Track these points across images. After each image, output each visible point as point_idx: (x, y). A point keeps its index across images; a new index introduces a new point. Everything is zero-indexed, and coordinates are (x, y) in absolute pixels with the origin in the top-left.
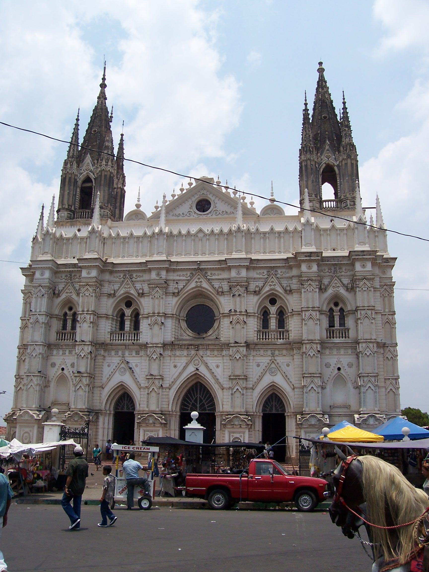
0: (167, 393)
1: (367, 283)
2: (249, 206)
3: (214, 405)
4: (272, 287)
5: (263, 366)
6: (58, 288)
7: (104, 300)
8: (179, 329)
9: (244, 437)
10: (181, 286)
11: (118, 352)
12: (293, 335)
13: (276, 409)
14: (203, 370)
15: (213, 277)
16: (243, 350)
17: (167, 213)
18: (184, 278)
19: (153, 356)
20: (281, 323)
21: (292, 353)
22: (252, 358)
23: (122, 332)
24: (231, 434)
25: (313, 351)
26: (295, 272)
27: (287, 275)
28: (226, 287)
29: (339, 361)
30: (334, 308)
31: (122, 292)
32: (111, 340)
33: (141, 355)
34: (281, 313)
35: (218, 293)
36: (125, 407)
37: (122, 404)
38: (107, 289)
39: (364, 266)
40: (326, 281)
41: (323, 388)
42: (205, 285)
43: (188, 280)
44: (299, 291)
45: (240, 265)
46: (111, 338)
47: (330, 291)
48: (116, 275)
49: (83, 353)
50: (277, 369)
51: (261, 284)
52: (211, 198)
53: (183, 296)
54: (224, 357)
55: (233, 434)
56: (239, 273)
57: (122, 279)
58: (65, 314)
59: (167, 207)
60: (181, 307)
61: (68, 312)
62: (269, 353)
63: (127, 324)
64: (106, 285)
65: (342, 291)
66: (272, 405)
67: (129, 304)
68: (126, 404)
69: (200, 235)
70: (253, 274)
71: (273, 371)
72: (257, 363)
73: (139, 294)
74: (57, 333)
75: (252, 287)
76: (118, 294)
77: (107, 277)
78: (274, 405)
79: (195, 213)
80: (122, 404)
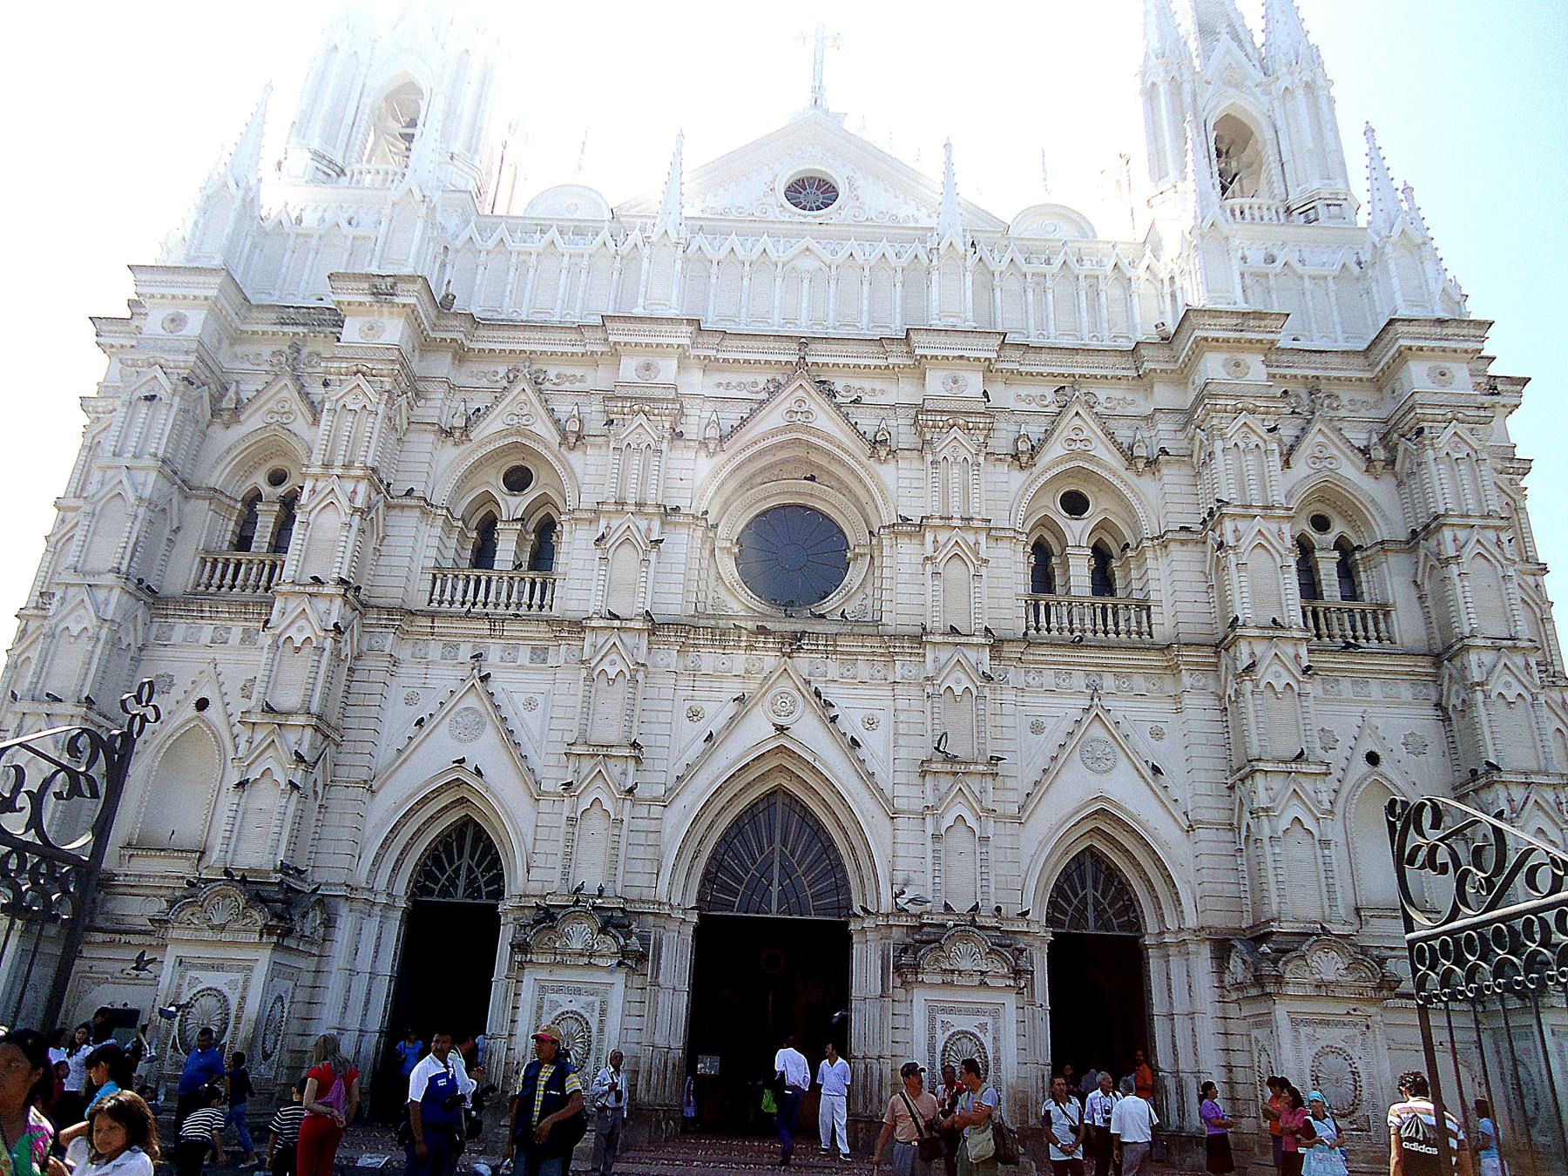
0: (653, 825)
3: (842, 886)
6: (237, 393)
7: (423, 443)
8: (712, 583)
9: (997, 1030)
11: (457, 647)
13: (1098, 917)
14: (809, 733)
18: (745, 394)
19: (605, 666)
22: (1010, 696)
23: (483, 574)
24: (940, 1017)
25: (1282, 670)
30: (1315, 536)
31: (498, 425)
32: (431, 601)
33: (551, 661)
36: (462, 883)
37: (449, 871)
38: (438, 406)
43: (762, 402)
45: (961, 357)
46: (432, 594)
48: (476, 367)
49: (300, 630)
50: (1118, 750)
51: (1035, 430)
54: (899, 689)
55: (946, 1017)
57: (504, 383)
58: (255, 498)
63: (506, 549)
64: (437, 393)
65: (1350, 471)
66: (1084, 900)
67: (518, 480)
68: (463, 873)
71: (1099, 754)
72: (1034, 719)
73: (564, 435)
74: (204, 561)
76: (480, 432)
78: (1090, 900)
80: (449, 871)
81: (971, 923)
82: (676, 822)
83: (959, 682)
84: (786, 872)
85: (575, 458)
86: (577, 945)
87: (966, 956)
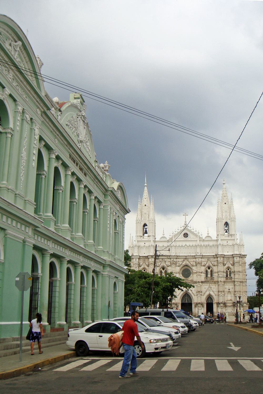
1: (238, 264)
2: (201, 236)
4: (209, 264)
5: (206, 289)
10: (181, 263)
12: (216, 279)
15: (190, 261)
16: (201, 284)
20: (212, 275)
22: (203, 286)
26: (216, 259)
28: (195, 264)
29: (229, 287)
30: (228, 271)
34: (211, 271)
35: (192, 266)
39: (237, 259)
41: (224, 295)
44: (217, 265)
47: (227, 266)
51: (205, 263)
52: (188, 233)
53: (182, 266)
56: (199, 260)
59: (174, 236)
62: (208, 284)
65: (230, 266)
69: (186, 246)
70: (203, 260)
73: (167, 266)
75: (203, 264)
76: (160, 266)
79: (183, 238)
81: (199, 303)
83: (199, 285)
87: (199, 305)
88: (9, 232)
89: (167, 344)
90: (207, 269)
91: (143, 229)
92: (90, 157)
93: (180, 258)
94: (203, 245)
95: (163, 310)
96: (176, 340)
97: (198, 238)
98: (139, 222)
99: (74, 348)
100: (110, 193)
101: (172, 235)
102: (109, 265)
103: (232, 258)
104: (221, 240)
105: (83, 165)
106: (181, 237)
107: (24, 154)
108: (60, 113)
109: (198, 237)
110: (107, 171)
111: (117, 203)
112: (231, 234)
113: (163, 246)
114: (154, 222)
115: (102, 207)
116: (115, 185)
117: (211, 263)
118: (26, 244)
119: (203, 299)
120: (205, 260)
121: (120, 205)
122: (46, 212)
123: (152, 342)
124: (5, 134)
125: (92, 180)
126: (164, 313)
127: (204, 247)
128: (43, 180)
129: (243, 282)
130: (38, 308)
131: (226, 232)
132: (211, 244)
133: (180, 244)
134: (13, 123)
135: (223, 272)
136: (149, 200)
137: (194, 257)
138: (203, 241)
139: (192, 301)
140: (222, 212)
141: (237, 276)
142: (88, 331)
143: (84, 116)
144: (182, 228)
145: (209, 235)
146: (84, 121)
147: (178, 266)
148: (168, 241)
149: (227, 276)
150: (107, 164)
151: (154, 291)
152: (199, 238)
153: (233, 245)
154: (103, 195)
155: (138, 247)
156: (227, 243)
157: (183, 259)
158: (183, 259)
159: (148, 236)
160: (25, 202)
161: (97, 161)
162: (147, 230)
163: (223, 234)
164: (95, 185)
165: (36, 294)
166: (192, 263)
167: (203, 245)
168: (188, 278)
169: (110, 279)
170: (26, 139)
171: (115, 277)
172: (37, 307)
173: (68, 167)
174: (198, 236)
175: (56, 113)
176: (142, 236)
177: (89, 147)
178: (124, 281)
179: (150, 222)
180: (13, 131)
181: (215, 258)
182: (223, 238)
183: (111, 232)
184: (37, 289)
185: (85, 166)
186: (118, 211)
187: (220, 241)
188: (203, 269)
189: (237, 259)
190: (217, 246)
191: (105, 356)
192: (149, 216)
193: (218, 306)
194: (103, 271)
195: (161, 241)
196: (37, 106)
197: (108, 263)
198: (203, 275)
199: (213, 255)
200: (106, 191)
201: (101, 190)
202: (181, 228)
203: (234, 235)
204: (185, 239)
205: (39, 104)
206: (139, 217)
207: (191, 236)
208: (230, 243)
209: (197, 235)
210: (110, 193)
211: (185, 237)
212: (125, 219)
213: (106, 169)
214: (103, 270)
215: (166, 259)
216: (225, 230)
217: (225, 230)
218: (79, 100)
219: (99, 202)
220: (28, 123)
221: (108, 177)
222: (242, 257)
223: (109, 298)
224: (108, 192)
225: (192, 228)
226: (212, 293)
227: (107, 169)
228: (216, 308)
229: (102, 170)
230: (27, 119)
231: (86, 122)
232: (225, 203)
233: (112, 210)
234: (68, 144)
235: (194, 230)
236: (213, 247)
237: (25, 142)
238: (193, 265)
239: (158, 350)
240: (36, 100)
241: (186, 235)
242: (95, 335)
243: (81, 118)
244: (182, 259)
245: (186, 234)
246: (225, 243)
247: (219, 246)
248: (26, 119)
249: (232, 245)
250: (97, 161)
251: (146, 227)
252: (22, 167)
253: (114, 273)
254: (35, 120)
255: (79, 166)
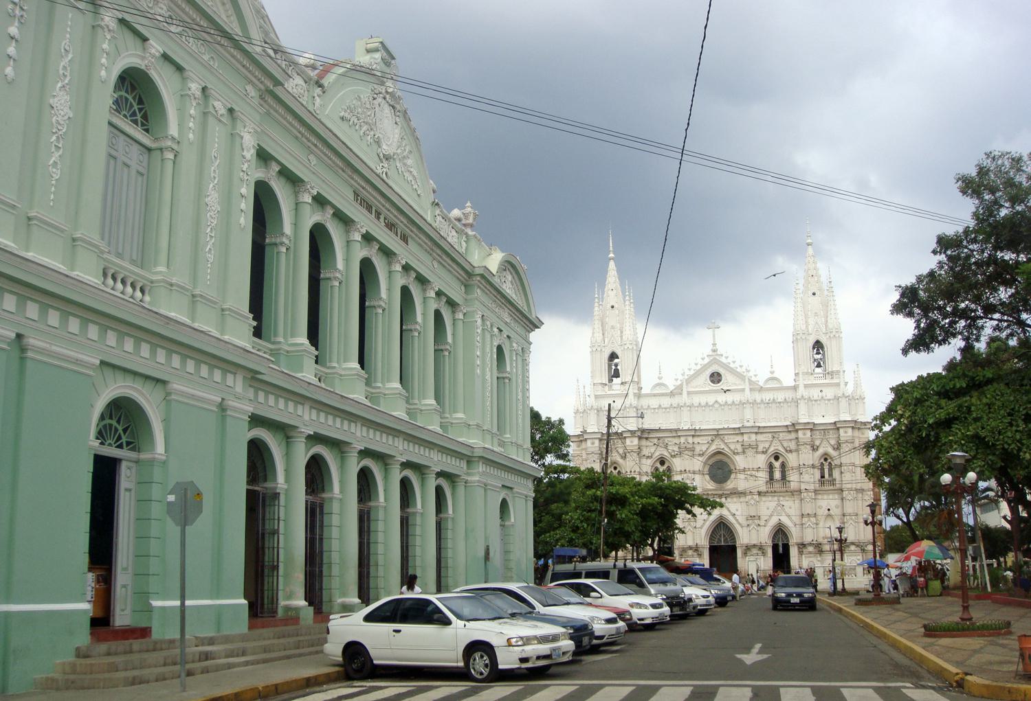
1: (849, 445)
2: (754, 379)
3: (734, 538)
4: (776, 448)
7: (644, 461)
10: (704, 449)
12: (793, 486)
15: (730, 441)
16: (756, 497)
17: (687, 384)
20: (784, 477)
21: (793, 499)
22: (762, 503)
26: (793, 435)
27: (788, 438)
28: (740, 450)
34: (783, 466)
40: (817, 443)
41: (817, 524)
42: (723, 446)
44: (797, 451)
47: (821, 451)
52: (721, 371)
56: (750, 438)
60: (705, 463)
61: (613, 471)
62: (776, 498)
69: (717, 406)
70: (760, 437)
73: (672, 456)
75: (760, 449)
76: (654, 457)
77: (644, 442)
81: (754, 546)
82: (703, 531)
83: (752, 502)
84: (724, 536)
85: (674, 460)
86: (690, 554)
87: (755, 551)
88: (175, 386)
89: (554, 649)
90: (773, 460)
91: (610, 366)
92: (419, 195)
93: (702, 435)
94: (759, 401)
95: (615, 565)
96: (608, 639)
97: (747, 383)
98: (599, 349)
99: (341, 659)
100: (479, 281)
101: (681, 377)
102: (482, 457)
103: (834, 431)
104: (806, 386)
105: (395, 216)
106: (704, 381)
107: (213, 198)
108: (318, 90)
109: (747, 380)
110: (471, 226)
111: (503, 303)
112: (830, 370)
113: (660, 406)
114: (635, 348)
115: (461, 316)
116: (494, 261)
117: (782, 445)
118: (230, 416)
119: (764, 536)
120: (766, 437)
121: (510, 308)
122: (293, 336)
123: (514, 644)
124: (158, 152)
125: (426, 250)
126: (617, 571)
127: (762, 406)
128: (283, 258)
129: (863, 490)
130: (278, 566)
131: (819, 366)
132: (780, 396)
133: (703, 399)
134: (179, 125)
135: (813, 466)
136: (621, 293)
137: (739, 431)
138: (759, 391)
139: (735, 542)
140: (806, 317)
141: (847, 477)
142: (369, 618)
143: (392, 95)
144: (707, 360)
145: (775, 375)
146: (393, 107)
147: (700, 455)
148: (672, 394)
149: (823, 477)
150: (469, 209)
151: (606, 520)
152: (750, 384)
153: (837, 398)
154: (463, 288)
155: (598, 411)
156: (820, 394)
157: (710, 438)
158: (710, 438)
159: (622, 383)
160: (223, 315)
161: (437, 204)
162: (619, 367)
163: (810, 371)
164: (435, 264)
165: (274, 534)
166: (732, 448)
167: (759, 401)
168: (724, 485)
169: (489, 492)
170: (216, 161)
171: (503, 486)
172: (276, 564)
173: (353, 221)
174: (746, 378)
175: (308, 91)
176: (607, 383)
177: (412, 170)
178: (530, 497)
179: (626, 347)
180: (179, 142)
181: (790, 432)
182: (812, 380)
183: (488, 377)
184: (276, 521)
185: (401, 218)
186: (506, 323)
187: (801, 388)
188: (761, 461)
189: (846, 432)
190: (796, 402)
191: (412, 678)
192: (622, 332)
193: (801, 553)
194: (468, 474)
195: (655, 395)
196: (246, 78)
197: (478, 453)
198: (763, 475)
199: (787, 426)
200: (469, 277)
201: (455, 276)
202: (703, 359)
203: (838, 372)
204: (714, 388)
205: (250, 71)
206: (599, 336)
207: (728, 381)
208: (829, 393)
209: (745, 377)
210: (479, 281)
211: (713, 382)
212: (530, 343)
213: (468, 222)
214: (469, 471)
215: (669, 439)
216: (815, 360)
217: (815, 360)
218: (378, 56)
219: (452, 304)
220: (220, 121)
221: (473, 243)
222: (859, 429)
223: (486, 538)
224: (474, 279)
225: (730, 360)
226: (786, 521)
227: (470, 221)
228: (797, 558)
229: (455, 225)
230: (216, 111)
231: (398, 107)
232: (814, 294)
233: (488, 323)
234: (347, 165)
235: (737, 365)
236: (785, 405)
237: (214, 169)
238: (736, 451)
239: (530, 663)
240: (241, 63)
241: (716, 377)
242: (386, 628)
243: (385, 98)
244: (707, 438)
245: (716, 374)
246: (815, 393)
247: (799, 401)
248: (214, 113)
249: (833, 398)
250: (437, 204)
251: (616, 361)
252: (209, 229)
253: (497, 478)
254: (242, 114)
255: (385, 219)
